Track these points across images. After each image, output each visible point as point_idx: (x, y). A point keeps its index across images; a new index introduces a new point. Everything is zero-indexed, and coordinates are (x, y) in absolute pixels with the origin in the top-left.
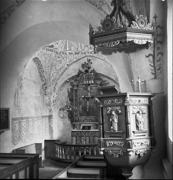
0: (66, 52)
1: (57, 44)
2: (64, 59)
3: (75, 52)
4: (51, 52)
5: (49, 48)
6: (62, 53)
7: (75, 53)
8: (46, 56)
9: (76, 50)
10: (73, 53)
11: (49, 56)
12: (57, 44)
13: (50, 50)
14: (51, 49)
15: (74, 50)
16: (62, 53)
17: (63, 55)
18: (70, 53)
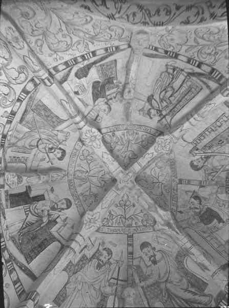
0: (24, 103)
1: (76, 93)
2: (5, 85)
3: (10, 133)
4: (67, 58)
5: (86, 63)
6: (30, 87)
7: (5, 133)
8: (75, 39)
9: (13, 140)
10: (8, 126)
11: (63, 46)
12: (76, 93)
13: (80, 60)
14: (81, 66)
15: (15, 134)
16: (30, 87)
17: (18, 89)
18: (13, 114)
